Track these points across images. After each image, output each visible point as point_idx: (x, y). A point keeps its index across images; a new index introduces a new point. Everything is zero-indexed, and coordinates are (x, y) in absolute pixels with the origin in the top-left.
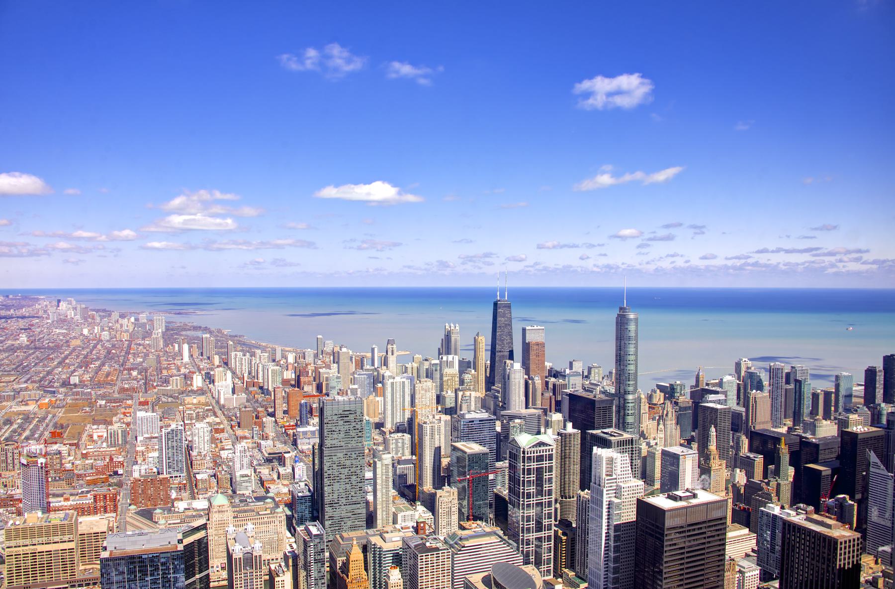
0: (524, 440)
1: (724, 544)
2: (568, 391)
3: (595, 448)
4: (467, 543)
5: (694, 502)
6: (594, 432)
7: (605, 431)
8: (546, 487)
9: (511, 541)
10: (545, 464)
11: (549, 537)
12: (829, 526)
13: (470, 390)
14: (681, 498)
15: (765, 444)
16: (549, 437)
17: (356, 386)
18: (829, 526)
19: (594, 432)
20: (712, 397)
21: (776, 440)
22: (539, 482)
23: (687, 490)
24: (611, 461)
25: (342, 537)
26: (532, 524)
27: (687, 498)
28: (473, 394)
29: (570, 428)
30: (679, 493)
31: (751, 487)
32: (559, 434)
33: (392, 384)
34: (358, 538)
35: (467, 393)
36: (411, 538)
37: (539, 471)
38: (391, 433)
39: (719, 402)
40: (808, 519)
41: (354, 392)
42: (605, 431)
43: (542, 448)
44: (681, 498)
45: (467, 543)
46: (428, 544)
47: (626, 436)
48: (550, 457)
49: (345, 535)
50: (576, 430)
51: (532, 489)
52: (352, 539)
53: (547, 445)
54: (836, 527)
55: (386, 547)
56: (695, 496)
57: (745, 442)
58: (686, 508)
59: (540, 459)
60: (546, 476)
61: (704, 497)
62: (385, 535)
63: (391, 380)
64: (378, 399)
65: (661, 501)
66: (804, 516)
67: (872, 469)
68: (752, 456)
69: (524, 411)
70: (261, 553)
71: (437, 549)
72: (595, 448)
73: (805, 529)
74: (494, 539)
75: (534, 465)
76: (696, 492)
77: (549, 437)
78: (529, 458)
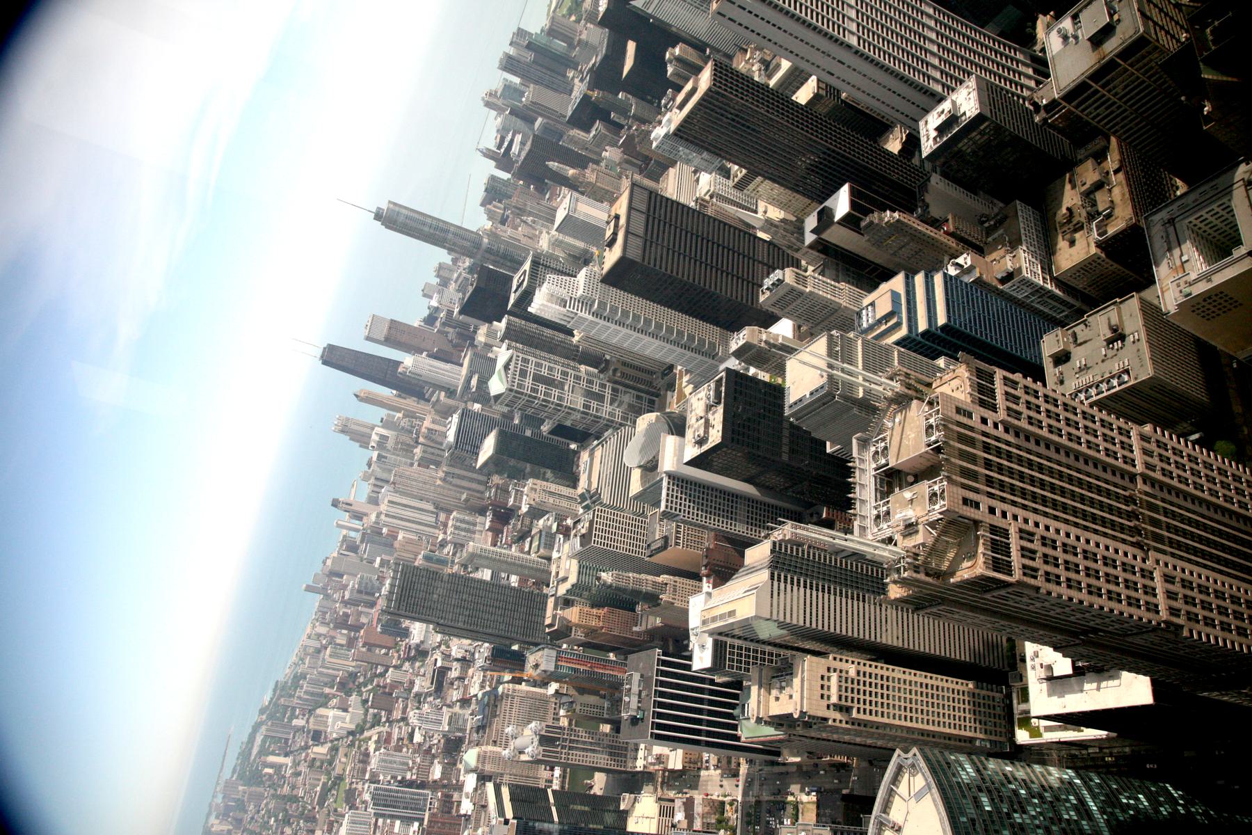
0: (497, 386)
1: (678, 204)
2: (456, 311)
3: (530, 309)
4: (594, 485)
5: (623, 221)
6: (512, 301)
7: (514, 288)
8: (558, 376)
9: (606, 434)
10: (531, 369)
11: (613, 390)
12: (694, 90)
13: (421, 426)
14: (615, 234)
15: (587, 114)
16: (502, 354)
17: (378, 560)
18: (694, 90)
19: (512, 301)
20: (515, 149)
21: (585, 99)
22: (549, 382)
23: (608, 223)
24: (552, 297)
25: (550, 626)
26: (594, 404)
27: (616, 226)
28: (427, 423)
29: (501, 326)
30: (609, 233)
31: (628, 147)
32: (502, 341)
33: (387, 515)
34: (555, 608)
35: (423, 430)
36: (573, 547)
37: (537, 378)
38: (445, 533)
39: (523, 143)
40: (681, 107)
41: (382, 564)
42: (514, 288)
43: (512, 364)
44: (615, 234)
45: (594, 485)
46: (583, 531)
47: (527, 266)
48: (525, 361)
49: (548, 621)
50: (504, 321)
51: (555, 392)
52: (554, 616)
53: (510, 360)
54: (696, 82)
55: (573, 579)
56: (617, 217)
57: (576, 133)
58: (627, 232)
59: (523, 373)
60: (544, 372)
61: (621, 207)
62: (561, 576)
63: (383, 517)
64: (400, 537)
65: (612, 256)
66: (675, 110)
67: (650, 11)
68: (593, 133)
69: (464, 371)
70: (544, 724)
71: (591, 522)
72: (530, 309)
73: (688, 117)
74: (598, 453)
75: (529, 382)
76: (613, 214)
77: (502, 354)
78: (520, 386)
